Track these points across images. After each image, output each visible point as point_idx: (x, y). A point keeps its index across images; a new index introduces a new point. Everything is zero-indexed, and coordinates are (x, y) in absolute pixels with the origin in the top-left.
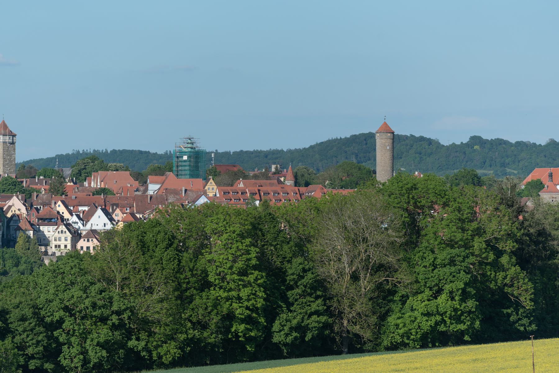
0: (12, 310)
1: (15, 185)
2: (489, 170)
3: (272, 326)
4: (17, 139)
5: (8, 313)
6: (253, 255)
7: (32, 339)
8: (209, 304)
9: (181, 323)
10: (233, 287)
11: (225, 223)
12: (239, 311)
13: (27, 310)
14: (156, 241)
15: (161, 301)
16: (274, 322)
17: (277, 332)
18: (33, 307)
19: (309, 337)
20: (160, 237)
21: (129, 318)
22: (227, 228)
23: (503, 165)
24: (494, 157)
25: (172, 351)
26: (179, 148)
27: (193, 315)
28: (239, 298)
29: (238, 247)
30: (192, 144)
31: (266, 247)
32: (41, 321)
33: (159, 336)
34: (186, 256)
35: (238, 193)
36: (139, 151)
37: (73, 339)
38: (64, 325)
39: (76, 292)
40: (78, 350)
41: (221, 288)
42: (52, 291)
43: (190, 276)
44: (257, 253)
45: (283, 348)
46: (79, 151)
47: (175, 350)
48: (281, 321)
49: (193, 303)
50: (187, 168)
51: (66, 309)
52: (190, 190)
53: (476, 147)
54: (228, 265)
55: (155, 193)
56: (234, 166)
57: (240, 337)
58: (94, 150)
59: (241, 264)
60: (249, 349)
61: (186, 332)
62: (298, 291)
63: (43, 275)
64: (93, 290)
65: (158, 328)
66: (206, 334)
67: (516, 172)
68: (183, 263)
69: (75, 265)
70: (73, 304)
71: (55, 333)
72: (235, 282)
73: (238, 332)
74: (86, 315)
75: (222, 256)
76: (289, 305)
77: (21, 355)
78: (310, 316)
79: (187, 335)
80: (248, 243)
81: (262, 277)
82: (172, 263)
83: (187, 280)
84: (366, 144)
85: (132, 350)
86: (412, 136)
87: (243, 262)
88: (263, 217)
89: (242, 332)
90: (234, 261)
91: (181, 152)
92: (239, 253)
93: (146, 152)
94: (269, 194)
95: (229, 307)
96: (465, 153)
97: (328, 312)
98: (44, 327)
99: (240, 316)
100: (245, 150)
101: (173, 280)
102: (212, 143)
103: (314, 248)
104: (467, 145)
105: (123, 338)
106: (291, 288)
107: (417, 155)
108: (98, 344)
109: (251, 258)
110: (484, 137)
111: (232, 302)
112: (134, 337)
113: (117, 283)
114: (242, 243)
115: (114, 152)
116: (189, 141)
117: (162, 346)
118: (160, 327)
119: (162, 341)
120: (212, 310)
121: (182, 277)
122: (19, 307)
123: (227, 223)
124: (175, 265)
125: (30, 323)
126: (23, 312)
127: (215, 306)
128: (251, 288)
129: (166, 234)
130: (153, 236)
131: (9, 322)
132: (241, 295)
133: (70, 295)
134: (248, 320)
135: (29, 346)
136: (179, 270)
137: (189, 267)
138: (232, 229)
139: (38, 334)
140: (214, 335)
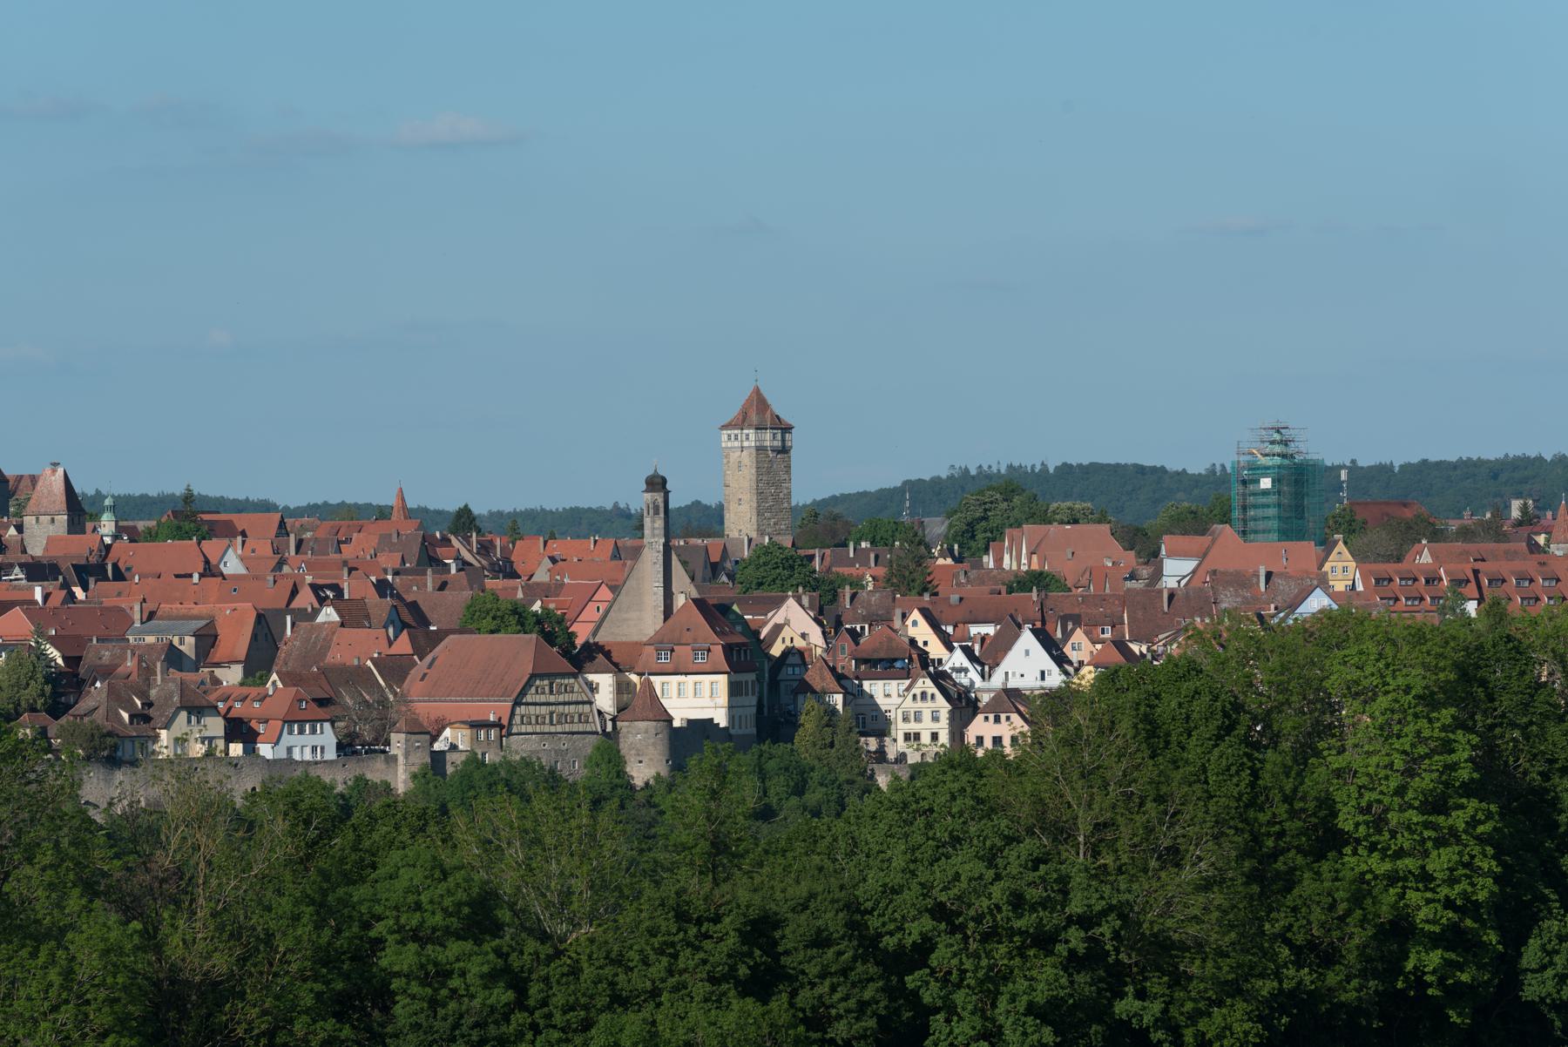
0: (790, 915)
1: (792, 567)
3: (1520, 955)
4: (794, 439)
5: (778, 923)
6: (1463, 754)
7: (845, 999)
8: (1340, 895)
9: (1261, 948)
10: (1406, 845)
11: (1381, 665)
12: (1426, 913)
13: (830, 915)
14: (1188, 718)
15: (1206, 886)
16: (1525, 943)
17: (1534, 971)
18: (847, 906)
20: (1199, 707)
21: (1116, 935)
22: (1388, 679)
25: (1237, 1028)
26: (1249, 458)
27: (1296, 925)
28: (1425, 877)
29: (1419, 732)
30: (1285, 443)
31: (1498, 731)
32: (869, 945)
33: (1202, 986)
35: (1415, 580)
36: (1135, 466)
37: (959, 997)
38: (933, 956)
39: (965, 863)
40: (974, 1028)
41: (1372, 848)
42: (899, 862)
43: (1285, 816)
44: (1474, 748)
45: (1553, 1015)
46: (967, 470)
47: (1247, 1026)
48: (1545, 940)
49: (1296, 892)
50: (1272, 512)
51: (939, 912)
52: (1281, 575)
54: (1393, 784)
55: (1183, 583)
56: (1405, 505)
57: (1430, 985)
58: (1010, 467)
59: (1427, 780)
60: (1454, 1018)
61: (1278, 976)
63: (873, 817)
64: (1015, 857)
65: (1198, 962)
66: (1332, 978)
68: (1266, 779)
69: (963, 790)
70: (959, 898)
71: (908, 979)
72: (1412, 832)
73: (1424, 973)
74: (995, 927)
75: (1374, 760)
77: (815, 1042)
79: (1281, 982)
80: (1449, 721)
81: (1489, 816)
82: (1235, 780)
83: (1277, 828)
85: (1124, 1025)
87: (1436, 775)
88: (1488, 646)
89: (1433, 972)
90: (1410, 773)
91: (1253, 467)
92: (1422, 750)
93: (1154, 470)
94: (1504, 581)
95: (1397, 902)
98: (877, 964)
99: (1427, 927)
100: (1433, 458)
101: (1236, 829)
102: (1343, 440)
105: (1099, 991)
109: (1455, 764)
111: (1404, 888)
112: (1130, 989)
113: (1081, 839)
114: (1430, 721)
115: (1066, 469)
116: (1277, 437)
117: (1209, 1015)
118: (1204, 960)
119: (1209, 999)
120: (1348, 913)
121: (1263, 818)
122: (807, 908)
123: (1387, 666)
124: (1243, 785)
125: (840, 953)
126: (820, 922)
127: (1357, 900)
128: (1457, 849)
129: (1216, 698)
130: (1180, 705)
131: (780, 949)
132: (1430, 868)
133: (950, 873)
134: (1451, 938)
135: (839, 1017)
136: (1255, 799)
137: (1281, 789)
138: (1400, 681)
140: (1355, 983)
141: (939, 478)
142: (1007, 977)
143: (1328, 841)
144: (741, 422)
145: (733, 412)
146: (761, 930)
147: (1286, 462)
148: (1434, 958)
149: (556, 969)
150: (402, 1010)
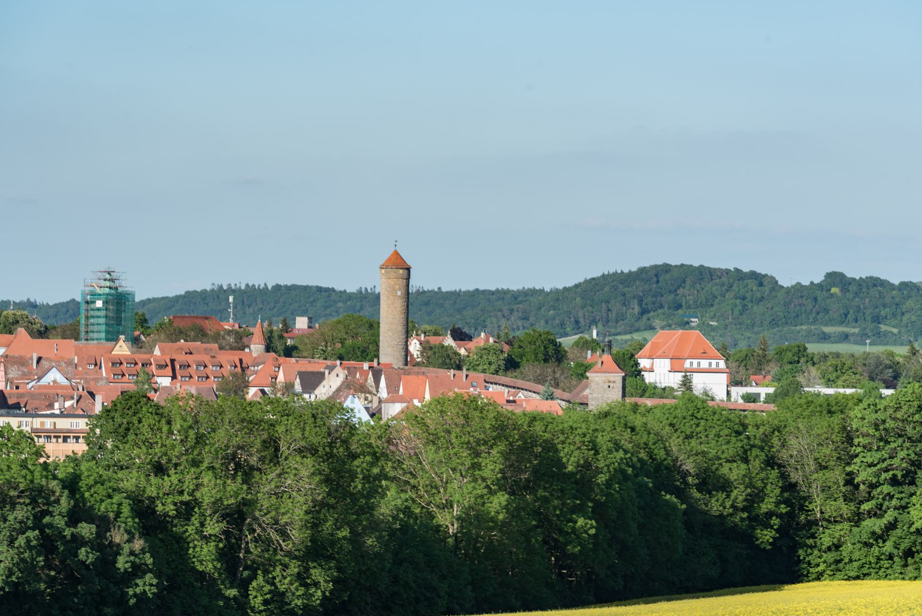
2: (854, 327)
23: (877, 319)
24: (862, 306)
26: (91, 288)
30: (112, 280)
36: (317, 287)
52: (48, 359)
53: (834, 290)
56: (207, 318)
58: (247, 285)
67: (895, 331)
84: (658, 282)
86: (737, 270)
91: (93, 294)
94: (189, 366)
96: (815, 299)
100: (481, 288)
104: (820, 286)
107: (738, 301)
110: (849, 275)
115: (277, 287)
116: (108, 276)
141: (206, 290)
147: (113, 291)
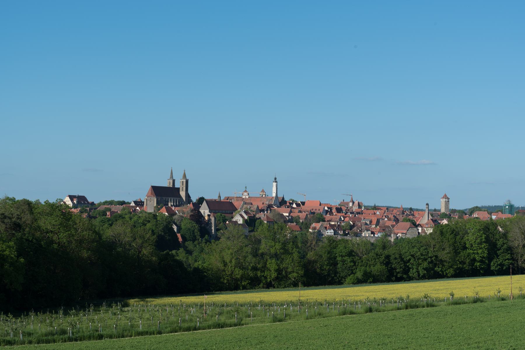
15: (448, 253)
19: (505, 268)
20: (448, 230)
28: (478, 253)
32: (402, 260)
34: (458, 237)
39: (415, 249)
51: (412, 255)
62: (502, 251)
66: (465, 266)
68: (457, 240)
76: (498, 256)
78: (505, 260)
90: (476, 239)
97: (513, 259)
103: (510, 235)
106: (499, 250)
108: (423, 268)
127: (468, 256)
136: (455, 242)
139: (401, 264)
142: (421, 264)
143: (465, 248)
144: (443, 198)
145: (442, 196)
146: (388, 257)
148: (478, 264)
149: (360, 261)
150: (339, 265)
